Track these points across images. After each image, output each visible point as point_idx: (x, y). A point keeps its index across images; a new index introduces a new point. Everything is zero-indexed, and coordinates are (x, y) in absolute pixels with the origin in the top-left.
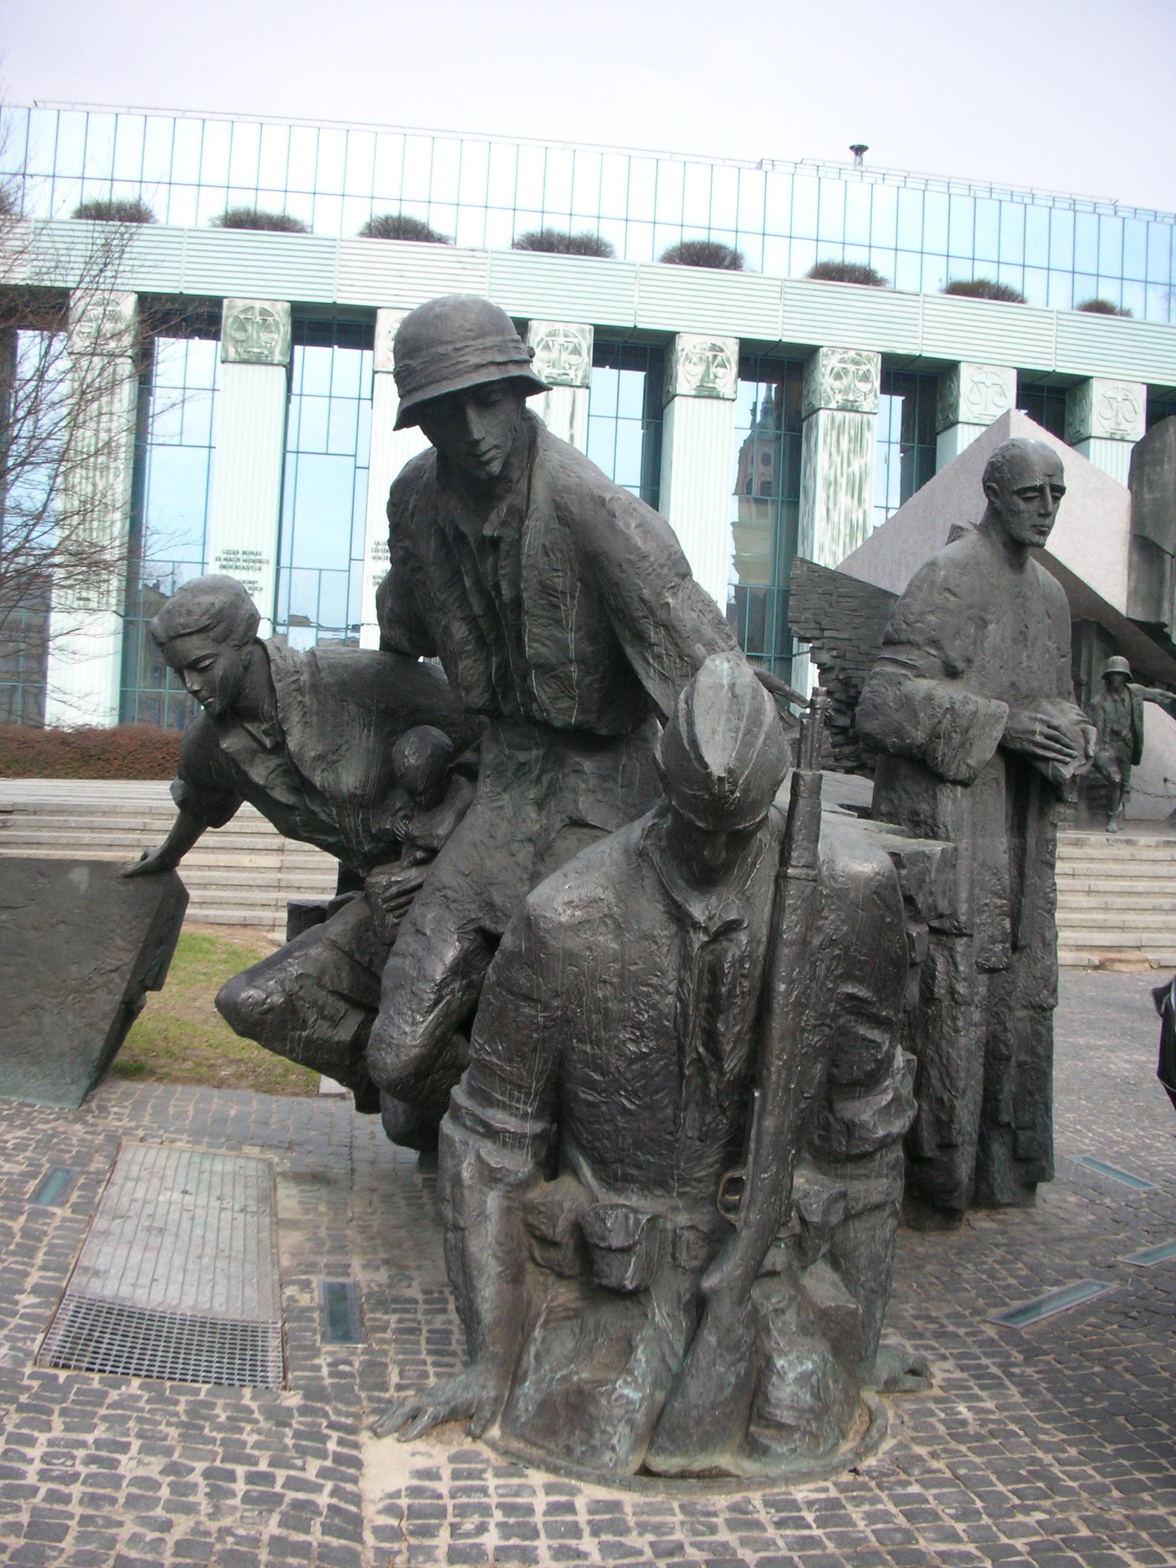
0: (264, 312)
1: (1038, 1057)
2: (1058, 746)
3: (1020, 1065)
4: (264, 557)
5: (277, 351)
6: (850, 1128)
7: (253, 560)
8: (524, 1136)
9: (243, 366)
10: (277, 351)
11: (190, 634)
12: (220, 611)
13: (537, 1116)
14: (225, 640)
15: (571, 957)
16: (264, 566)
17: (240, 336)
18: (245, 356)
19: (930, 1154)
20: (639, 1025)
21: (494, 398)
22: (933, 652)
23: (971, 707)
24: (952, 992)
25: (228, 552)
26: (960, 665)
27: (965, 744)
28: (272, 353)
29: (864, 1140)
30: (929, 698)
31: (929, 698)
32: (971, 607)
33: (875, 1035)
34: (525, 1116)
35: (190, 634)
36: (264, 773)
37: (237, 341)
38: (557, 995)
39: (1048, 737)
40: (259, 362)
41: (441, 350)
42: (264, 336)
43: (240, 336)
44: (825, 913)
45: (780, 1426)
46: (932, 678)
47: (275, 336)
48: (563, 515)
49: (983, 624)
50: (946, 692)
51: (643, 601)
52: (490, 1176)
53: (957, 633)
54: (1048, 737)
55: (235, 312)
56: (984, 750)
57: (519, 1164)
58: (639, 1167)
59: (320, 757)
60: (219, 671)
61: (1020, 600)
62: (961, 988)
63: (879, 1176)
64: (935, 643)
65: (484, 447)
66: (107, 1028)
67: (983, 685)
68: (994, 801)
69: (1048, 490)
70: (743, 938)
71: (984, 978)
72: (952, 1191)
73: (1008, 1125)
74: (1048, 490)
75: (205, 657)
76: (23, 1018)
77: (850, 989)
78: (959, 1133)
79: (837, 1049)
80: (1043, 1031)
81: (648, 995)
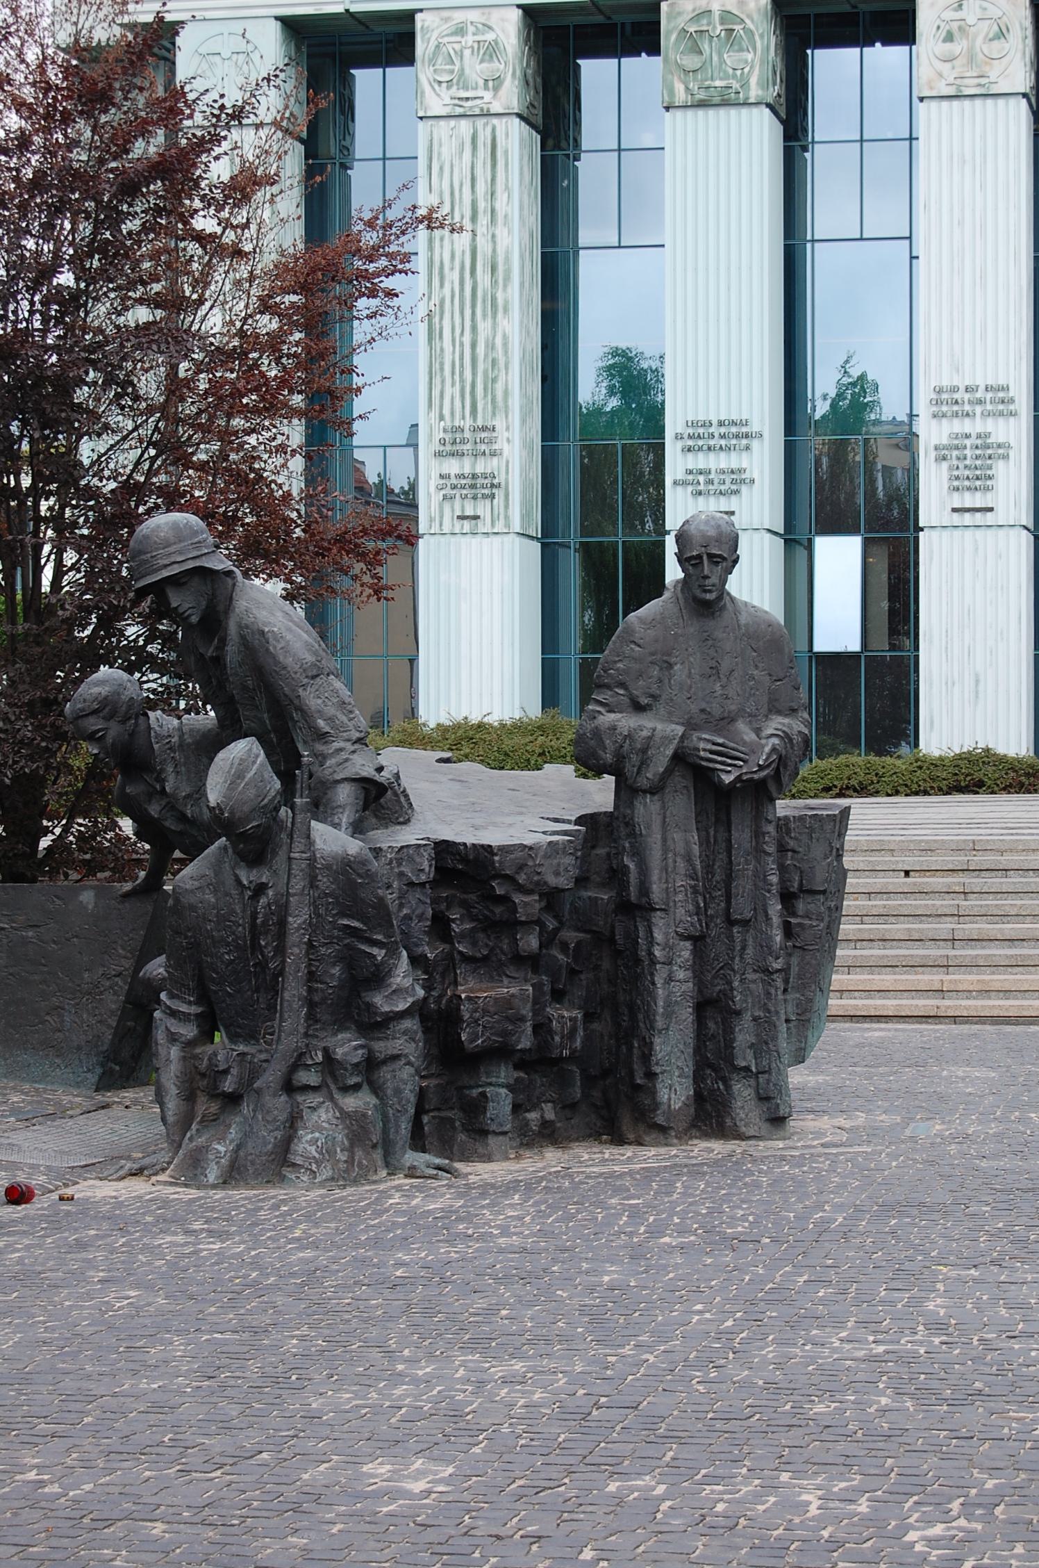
0: (726, 16)
1: (769, 1012)
2: (720, 759)
3: (755, 1019)
4: (755, 427)
5: (753, 81)
6: (370, 1007)
7: (737, 434)
8: (189, 1014)
9: (701, 113)
10: (753, 81)
11: (87, 715)
12: (106, 698)
13: (196, 1003)
14: (112, 717)
15: (193, 908)
16: (755, 444)
17: (691, 62)
18: (702, 95)
19: (639, 1081)
20: (228, 944)
21: (183, 580)
22: (621, 692)
23: (645, 733)
24: (650, 953)
25: (694, 424)
26: (644, 701)
27: (644, 764)
28: (745, 85)
29: (376, 1014)
30: (614, 728)
31: (614, 728)
32: (652, 654)
33: (375, 951)
34: (190, 1003)
35: (87, 715)
36: (158, 808)
37: (686, 72)
38: (189, 930)
39: (712, 752)
40: (725, 103)
41: (144, 557)
42: (730, 59)
43: (691, 62)
44: (320, 878)
45: (294, 1165)
46: (620, 712)
47: (750, 57)
48: (244, 642)
49: (670, 666)
50: (626, 722)
51: (286, 695)
52: (173, 1038)
53: (640, 675)
54: (712, 752)
55: (681, 22)
56: (660, 763)
57: (189, 1031)
58: (239, 1027)
59: (188, 796)
60: (109, 740)
61: (710, 642)
62: (657, 953)
63: (394, 1038)
64: (622, 685)
65: (181, 610)
66: (114, 1024)
67: (670, 713)
68: (681, 804)
69: (705, 557)
70: (271, 893)
71: (688, 944)
72: (655, 1110)
73: (747, 1069)
74: (705, 557)
75: (99, 730)
76: (48, 1018)
77: (345, 922)
78: (657, 1064)
79: (351, 959)
80: (773, 991)
81: (230, 927)
